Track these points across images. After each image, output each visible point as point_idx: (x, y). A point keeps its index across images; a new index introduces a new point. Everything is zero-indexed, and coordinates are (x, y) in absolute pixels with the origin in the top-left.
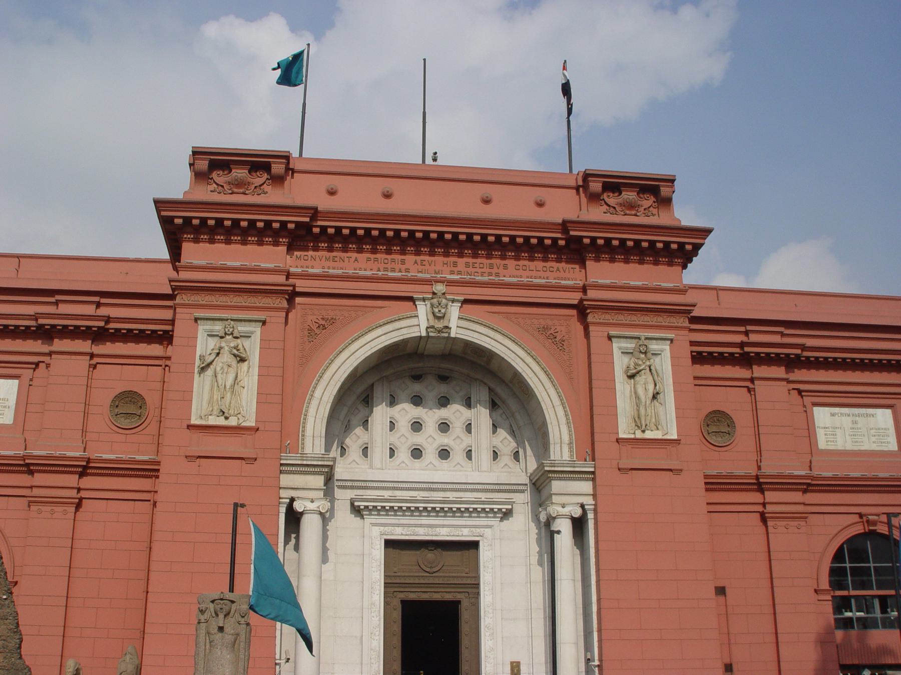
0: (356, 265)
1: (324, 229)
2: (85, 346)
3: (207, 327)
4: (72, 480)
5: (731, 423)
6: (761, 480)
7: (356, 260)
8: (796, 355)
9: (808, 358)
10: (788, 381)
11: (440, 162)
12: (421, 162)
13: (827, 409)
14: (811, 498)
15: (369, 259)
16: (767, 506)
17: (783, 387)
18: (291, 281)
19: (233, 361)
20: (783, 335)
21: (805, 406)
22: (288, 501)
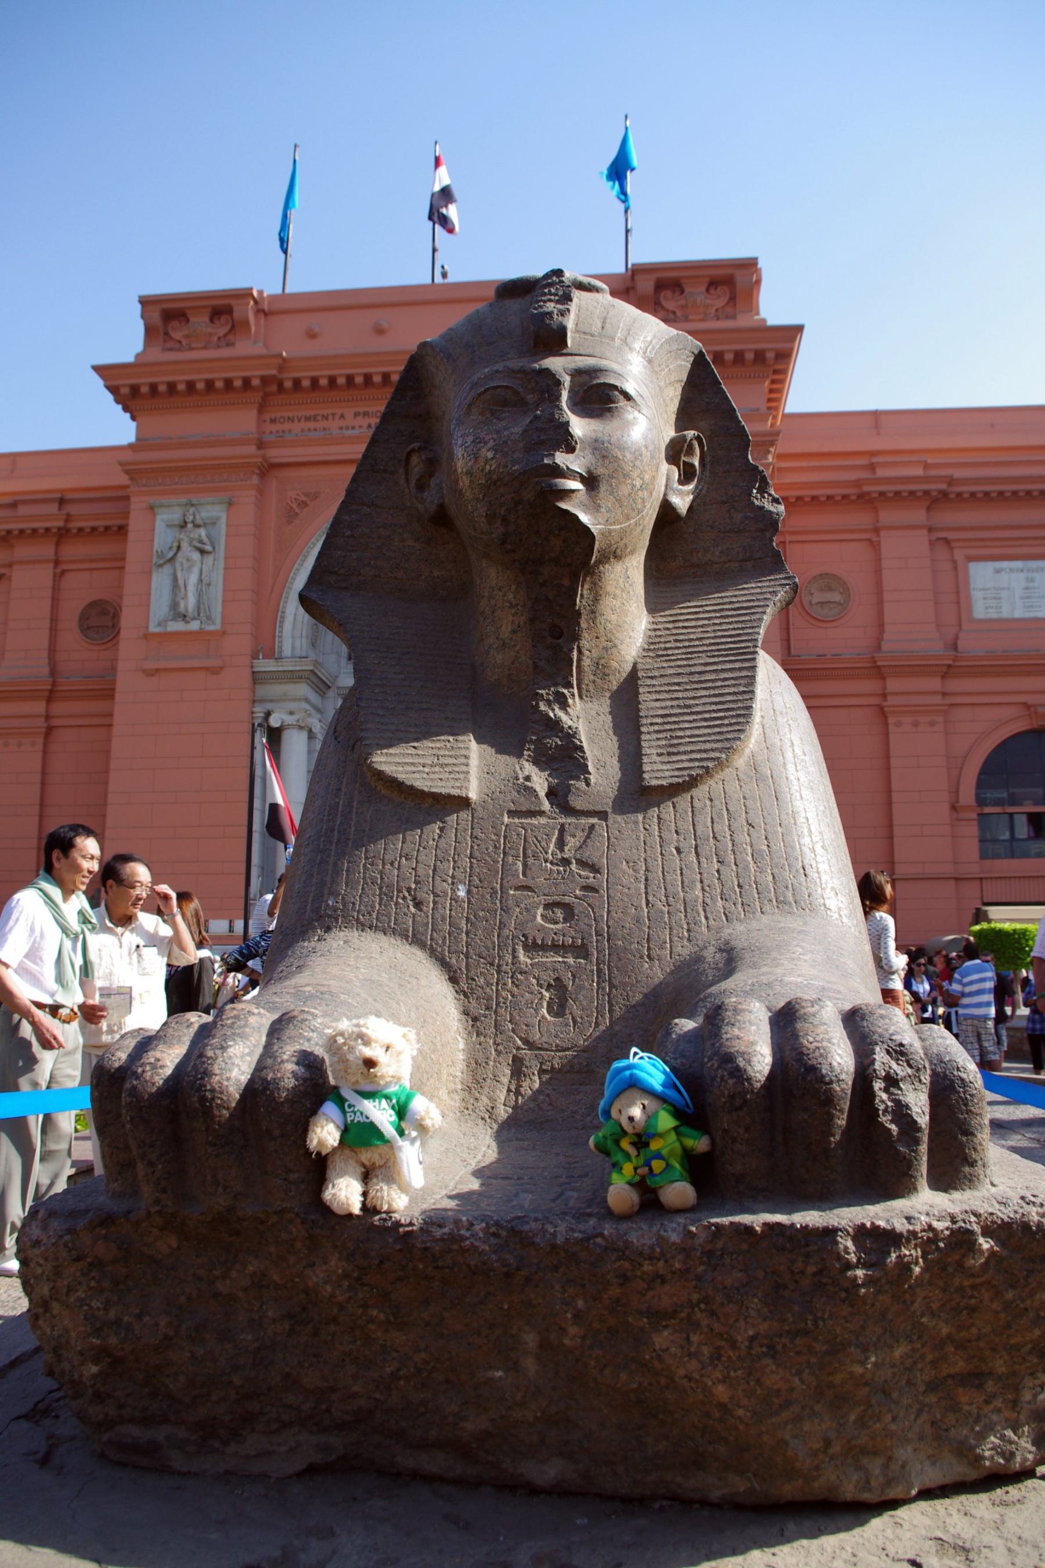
0: (343, 423)
1: (297, 382)
2: (47, 550)
3: (165, 517)
4: (40, 707)
5: (846, 590)
6: (879, 663)
7: (342, 416)
8: (940, 492)
9: (959, 495)
10: (930, 530)
11: (451, 279)
12: (429, 281)
13: (990, 566)
14: (955, 685)
15: (356, 415)
16: (889, 698)
17: (923, 536)
18: (260, 452)
19: (196, 556)
20: (926, 466)
21: (954, 562)
22: (262, 715)
